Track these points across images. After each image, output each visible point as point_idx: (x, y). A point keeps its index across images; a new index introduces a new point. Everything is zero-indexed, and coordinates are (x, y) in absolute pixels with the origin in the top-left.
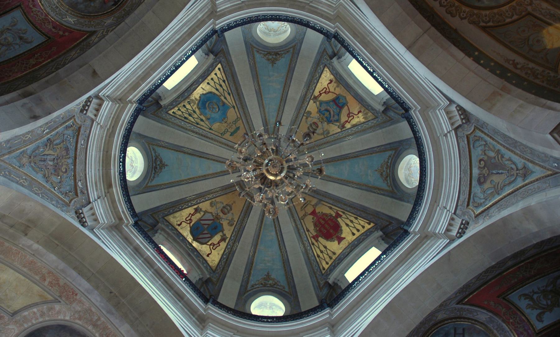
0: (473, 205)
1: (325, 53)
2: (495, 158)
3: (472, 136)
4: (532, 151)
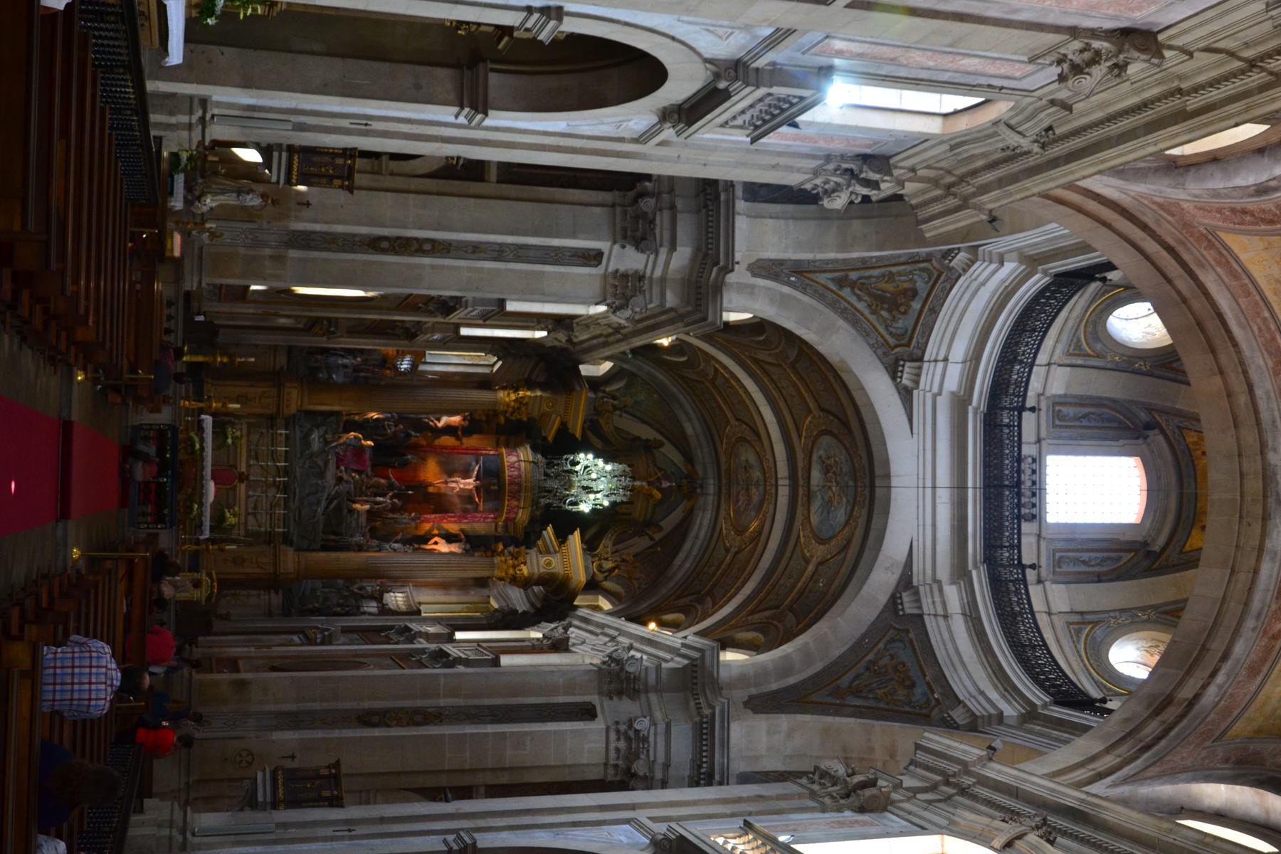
0: (931, 272)
1: (1156, 565)
2: (882, 308)
3: (902, 342)
4: (821, 298)
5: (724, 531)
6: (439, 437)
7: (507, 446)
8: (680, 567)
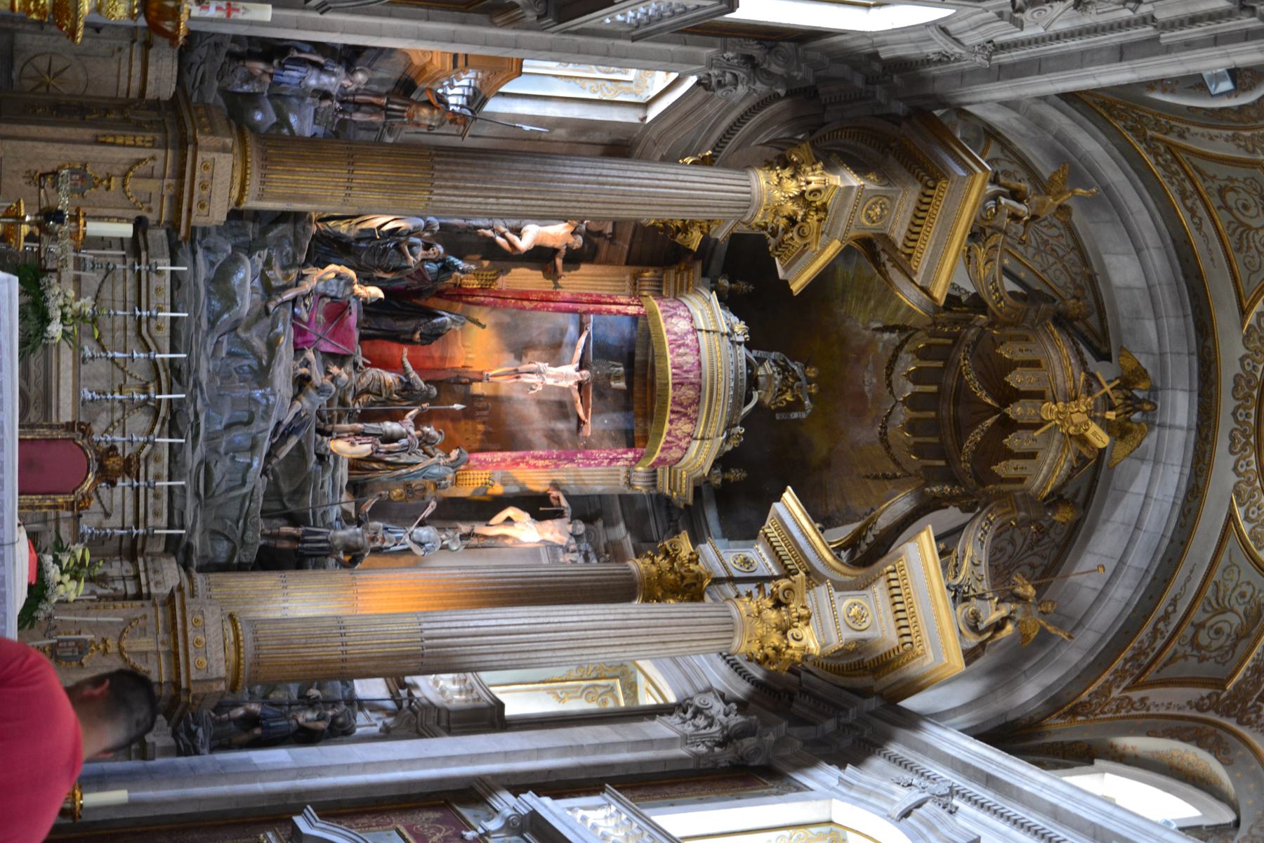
5: (1245, 528)
6: (505, 271)
7: (658, 294)
8: (1102, 595)
